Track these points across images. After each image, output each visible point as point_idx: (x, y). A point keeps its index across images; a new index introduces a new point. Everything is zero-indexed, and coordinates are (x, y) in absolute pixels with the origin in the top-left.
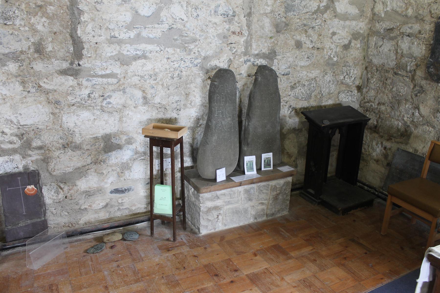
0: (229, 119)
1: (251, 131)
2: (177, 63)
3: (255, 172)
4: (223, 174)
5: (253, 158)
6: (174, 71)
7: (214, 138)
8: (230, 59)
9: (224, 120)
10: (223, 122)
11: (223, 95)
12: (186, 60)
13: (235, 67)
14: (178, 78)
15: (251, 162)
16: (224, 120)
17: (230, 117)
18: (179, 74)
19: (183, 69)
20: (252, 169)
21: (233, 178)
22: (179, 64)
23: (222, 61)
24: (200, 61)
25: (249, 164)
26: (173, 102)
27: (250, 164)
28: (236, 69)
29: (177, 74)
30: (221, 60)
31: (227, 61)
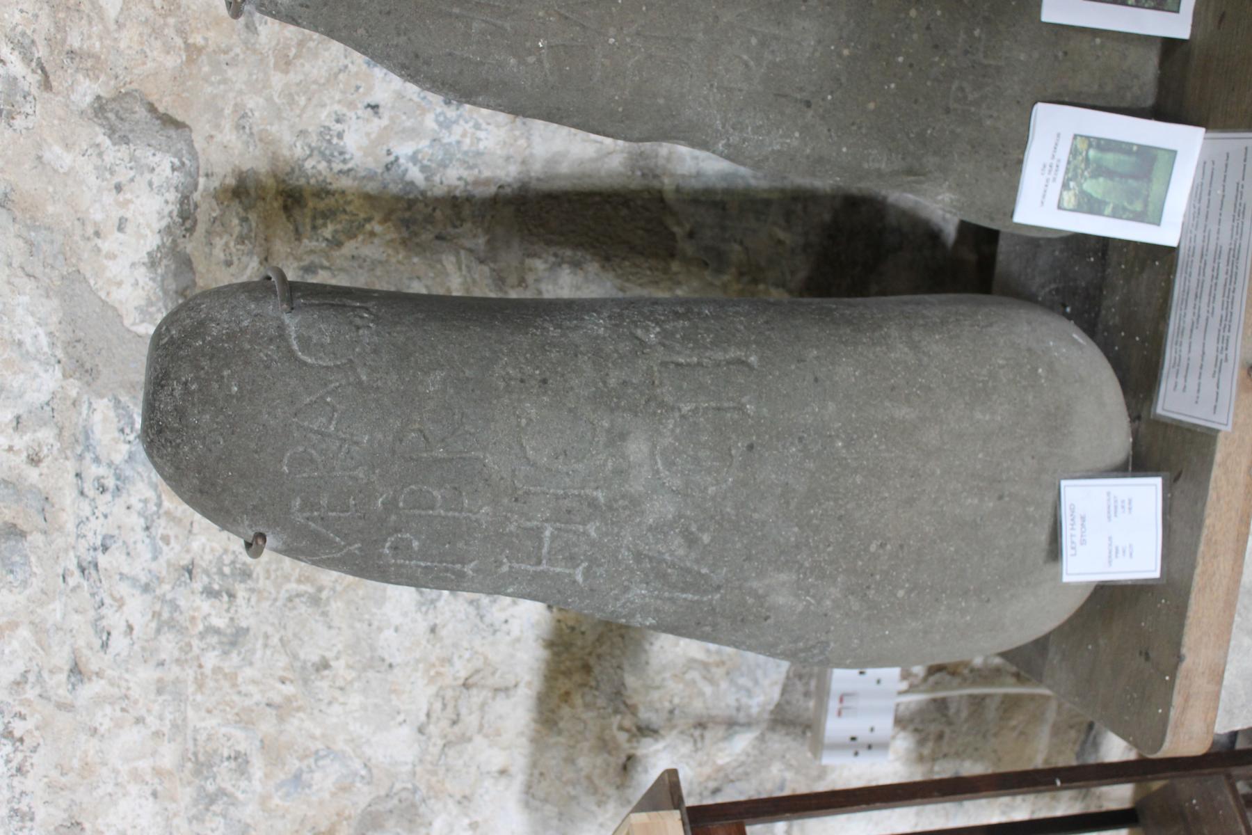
0: (637, 448)
1: (795, 140)
2: (120, 603)
3: (1186, 142)
4: (1113, 509)
5: (1055, 130)
6: (182, 631)
7: (782, 599)
8: (100, 108)
9: (635, 502)
10: (661, 508)
11: (391, 505)
12: (96, 529)
13: (172, 61)
14: (241, 591)
15: (1089, 157)
16: (635, 502)
17: (618, 437)
18: (209, 593)
19: (173, 553)
20: (1149, 163)
21: (1175, 400)
22: (123, 589)
23: (109, 198)
24: (103, 406)
25: (1095, 187)
26: (422, 626)
27: (1100, 171)
28: (193, 52)
29: (205, 605)
30: (101, 209)
31: (114, 154)
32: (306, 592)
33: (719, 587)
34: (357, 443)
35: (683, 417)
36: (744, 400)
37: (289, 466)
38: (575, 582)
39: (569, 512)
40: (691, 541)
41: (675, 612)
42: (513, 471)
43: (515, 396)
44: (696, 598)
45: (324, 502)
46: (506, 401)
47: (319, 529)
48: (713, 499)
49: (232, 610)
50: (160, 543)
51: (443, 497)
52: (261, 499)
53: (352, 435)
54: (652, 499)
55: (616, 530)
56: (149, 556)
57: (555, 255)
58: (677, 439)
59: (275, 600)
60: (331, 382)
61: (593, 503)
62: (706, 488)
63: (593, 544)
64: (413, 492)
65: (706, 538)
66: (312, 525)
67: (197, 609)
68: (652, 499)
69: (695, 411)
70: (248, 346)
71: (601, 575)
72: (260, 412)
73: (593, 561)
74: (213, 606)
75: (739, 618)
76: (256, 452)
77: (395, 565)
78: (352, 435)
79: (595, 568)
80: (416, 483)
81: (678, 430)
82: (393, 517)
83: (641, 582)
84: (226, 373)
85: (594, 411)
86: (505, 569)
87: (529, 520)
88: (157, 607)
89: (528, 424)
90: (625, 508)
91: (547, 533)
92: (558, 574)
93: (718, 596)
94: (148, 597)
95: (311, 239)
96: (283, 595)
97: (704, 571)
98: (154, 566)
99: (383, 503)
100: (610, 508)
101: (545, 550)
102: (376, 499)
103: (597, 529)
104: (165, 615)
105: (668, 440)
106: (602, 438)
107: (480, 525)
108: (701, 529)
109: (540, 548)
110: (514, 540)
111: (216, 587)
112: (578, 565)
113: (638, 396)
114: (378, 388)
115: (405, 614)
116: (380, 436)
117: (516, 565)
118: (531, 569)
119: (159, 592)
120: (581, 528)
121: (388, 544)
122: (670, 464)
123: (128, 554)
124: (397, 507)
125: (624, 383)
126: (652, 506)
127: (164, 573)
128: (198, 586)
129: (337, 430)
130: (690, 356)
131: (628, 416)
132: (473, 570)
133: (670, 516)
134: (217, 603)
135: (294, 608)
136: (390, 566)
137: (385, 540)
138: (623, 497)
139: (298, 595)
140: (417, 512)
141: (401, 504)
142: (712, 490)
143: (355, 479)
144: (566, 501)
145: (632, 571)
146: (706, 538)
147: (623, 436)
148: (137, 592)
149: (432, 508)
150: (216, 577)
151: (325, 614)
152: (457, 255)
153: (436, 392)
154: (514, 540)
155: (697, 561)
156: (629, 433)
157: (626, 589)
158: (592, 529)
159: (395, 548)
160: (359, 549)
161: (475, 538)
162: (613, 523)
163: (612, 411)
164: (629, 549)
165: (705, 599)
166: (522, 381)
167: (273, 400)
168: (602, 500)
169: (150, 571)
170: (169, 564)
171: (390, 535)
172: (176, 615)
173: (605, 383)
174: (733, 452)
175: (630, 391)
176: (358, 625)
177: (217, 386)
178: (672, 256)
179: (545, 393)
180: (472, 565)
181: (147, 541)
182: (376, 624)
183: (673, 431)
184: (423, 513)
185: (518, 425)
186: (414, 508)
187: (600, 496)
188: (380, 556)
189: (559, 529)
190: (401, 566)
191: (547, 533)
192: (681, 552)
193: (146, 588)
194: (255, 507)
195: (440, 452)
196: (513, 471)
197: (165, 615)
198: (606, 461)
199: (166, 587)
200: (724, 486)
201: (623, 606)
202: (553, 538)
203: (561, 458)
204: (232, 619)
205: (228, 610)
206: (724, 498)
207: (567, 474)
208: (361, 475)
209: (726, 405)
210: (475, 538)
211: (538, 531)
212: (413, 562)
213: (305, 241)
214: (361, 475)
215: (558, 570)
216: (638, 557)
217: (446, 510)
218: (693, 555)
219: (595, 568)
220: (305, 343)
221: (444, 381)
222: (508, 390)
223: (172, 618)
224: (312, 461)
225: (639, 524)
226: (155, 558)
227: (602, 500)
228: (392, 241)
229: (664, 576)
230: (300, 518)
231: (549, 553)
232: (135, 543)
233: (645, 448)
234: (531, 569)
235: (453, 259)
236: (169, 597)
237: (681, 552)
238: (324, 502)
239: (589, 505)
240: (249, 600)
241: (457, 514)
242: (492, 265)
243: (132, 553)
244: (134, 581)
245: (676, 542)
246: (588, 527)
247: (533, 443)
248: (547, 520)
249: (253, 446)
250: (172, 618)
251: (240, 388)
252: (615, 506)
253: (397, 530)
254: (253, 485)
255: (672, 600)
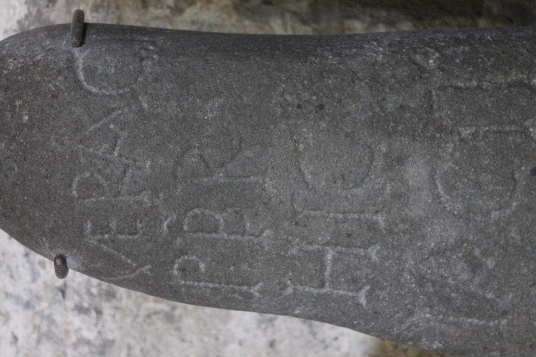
0: (415, 172)
6: (59, 342)
9: (416, 227)
10: (443, 232)
11: (176, 228)
14: (107, 308)
16: (416, 227)
18: (80, 309)
26: (262, 341)
29: (77, 321)
32: (162, 311)
33: (505, 313)
34: (140, 168)
35: (463, 141)
36: (527, 123)
37: (78, 191)
38: (358, 304)
39: (349, 236)
40: (475, 266)
41: (460, 336)
42: (292, 195)
43: (292, 122)
44: (482, 323)
45: (113, 225)
46: (284, 127)
47: (112, 251)
48: (497, 223)
49: (100, 325)
50: (38, 268)
51: (225, 221)
52: (54, 221)
53: (135, 161)
54: (432, 223)
55: (397, 254)
56: (29, 278)
57: (372, 16)
58: (456, 162)
59: (136, 316)
60: (114, 110)
61: (373, 227)
62: (489, 212)
63: (374, 267)
64: (195, 216)
65: (490, 263)
66: (105, 247)
67: (70, 323)
68: (432, 223)
69: (475, 135)
70: (38, 78)
71: (384, 298)
72: (49, 139)
73: (375, 285)
74: (83, 321)
75: (528, 344)
76: (47, 177)
77: (185, 286)
78: (135, 161)
79: (377, 292)
80: (198, 207)
81: (458, 154)
82: (179, 240)
83: (424, 306)
84: (18, 103)
85: (371, 135)
86: (290, 291)
87: (310, 243)
88: (37, 321)
89: (305, 149)
90: (405, 232)
91: (329, 257)
92: (341, 296)
93: (504, 322)
94: (29, 313)
95: (156, 7)
96: (143, 312)
97: (490, 296)
98: (34, 287)
99: (169, 227)
100: (390, 232)
101: (327, 273)
102: (162, 222)
103: (378, 252)
104: (44, 328)
105: (447, 166)
106: (379, 163)
107: (263, 248)
108: (484, 254)
109: (322, 269)
110: (297, 262)
111: (86, 305)
112: (361, 288)
113: (415, 120)
114: (158, 114)
115: (247, 331)
116: (161, 161)
117: (300, 288)
118: (315, 291)
119: (38, 308)
120: (362, 252)
121: (176, 266)
122: (450, 188)
123: (12, 276)
124: (181, 228)
125: (402, 107)
126: (433, 230)
127: (42, 293)
128: (70, 303)
129: (120, 156)
130: (470, 80)
131: (406, 140)
132: (260, 292)
133: (452, 240)
134: (86, 318)
135: (152, 324)
136: (181, 286)
137: (173, 262)
138: (403, 221)
139: (156, 313)
140: (201, 235)
141: (186, 228)
142: (495, 215)
143: (141, 203)
144: (346, 225)
145: (415, 295)
146: (490, 263)
147: (401, 160)
148: (20, 308)
149: (216, 232)
150: (86, 297)
151: (178, 329)
152: (283, 17)
153: (214, 119)
154: (297, 262)
155: (482, 286)
156: (407, 157)
157: (410, 313)
158: (373, 253)
159: (183, 269)
160: (150, 270)
161: (257, 261)
162: (393, 247)
163: (389, 135)
164: (411, 273)
165: (492, 324)
166: (299, 107)
167: (60, 127)
168: (382, 224)
169: (30, 291)
170: (46, 285)
171: (177, 257)
172: (53, 328)
173: (382, 107)
174: (517, 176)
175: (408, 115)
176: (206, 339)
177: (10, 116)
178: (479, 14)
179: (322, 118)
180: (258, 286)
181: (27, 265)
182: (222, 339)
183: (452, 155)
184: (207, 236)
185: (296, 150)
186: (197, 231)
187: (380, 219)
188: (170, 277)
189: (340, 253)
190: (191, 287)
191: (329, 257)
192: (465, 276)
193: (28, 305)
194: (51, 230)
195: (220, 177)
196: (292, 195)
197: (44, 328)
198: (385, 184)
199: (44, 305)
200: (508, 211)
201: (408, 329)
202: (335, 261)
203: (340, 182)
204: (100, 333)
205: (96, 325)
206: (508, 223)
207: (346, 197)
208: (146, 199)
209: (508, 128)
210: (257, 261)
211: (320, 257)
212: (202, 284)
213: (151, 9)
214: (146, 199)
215: (341, 292)
216: (421, 280)
217: (229, 234)
218: (477, 280)
219: (377, 292)
220: (90, 72)
221: (222, 108)
222: (285, 115)
223: (49, 331)
224: (98, 185)
225: (420, 248)
226: (34, 280)
227: (382, 224)
228: (226, 7)
229: (449, 300)
230: (93, 241)
231: (331, 275)
232: (17, 267)
233: (424, 172)
234: (315, 291)
235: (279, 21)
236: (46, 313)
237: (465, 276)
238: (113, 225)
239: (369, 229)
240: (114, 316)
241: (239, 237)
242: (314, 26)
243: (15, 276)
244: (17, 299)
245: (459, 267)
246: (370, 250)
247: (311, 168)
248: (327, 244)
249: (43, 171)
250: (49, 331)
251: (30, 117)
252: (396, 230)
253: (183, 252)
254: (46, 209)
255: (458, 325)
